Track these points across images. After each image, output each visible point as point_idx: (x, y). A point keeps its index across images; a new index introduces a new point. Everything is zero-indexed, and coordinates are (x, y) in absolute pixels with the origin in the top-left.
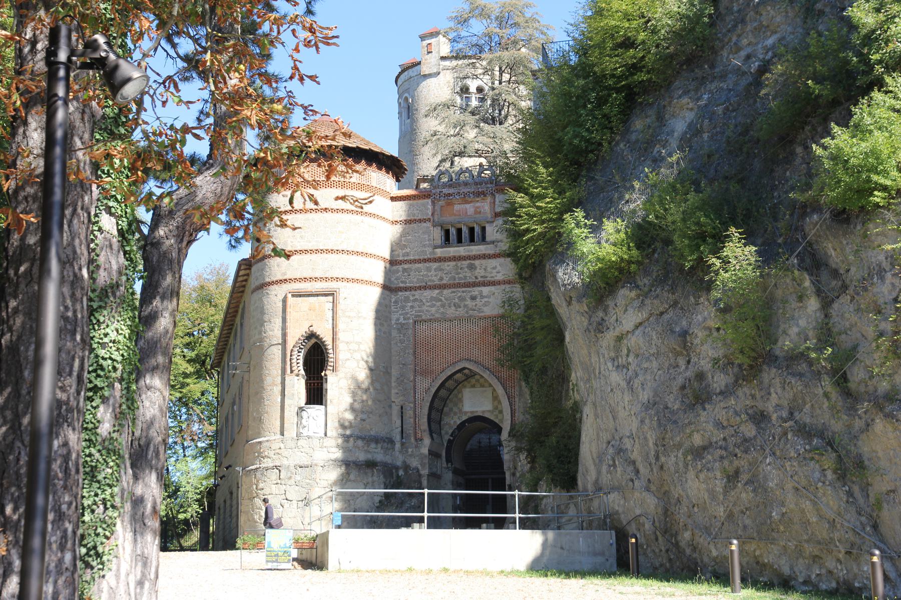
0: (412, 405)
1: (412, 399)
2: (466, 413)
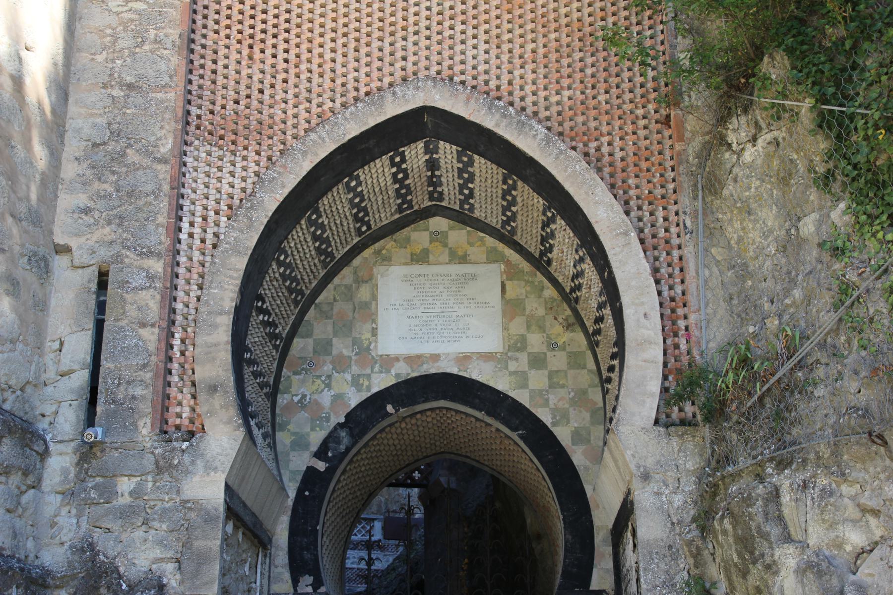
0: (157, 266)
1: (159, 237)
2: (388, 362)
